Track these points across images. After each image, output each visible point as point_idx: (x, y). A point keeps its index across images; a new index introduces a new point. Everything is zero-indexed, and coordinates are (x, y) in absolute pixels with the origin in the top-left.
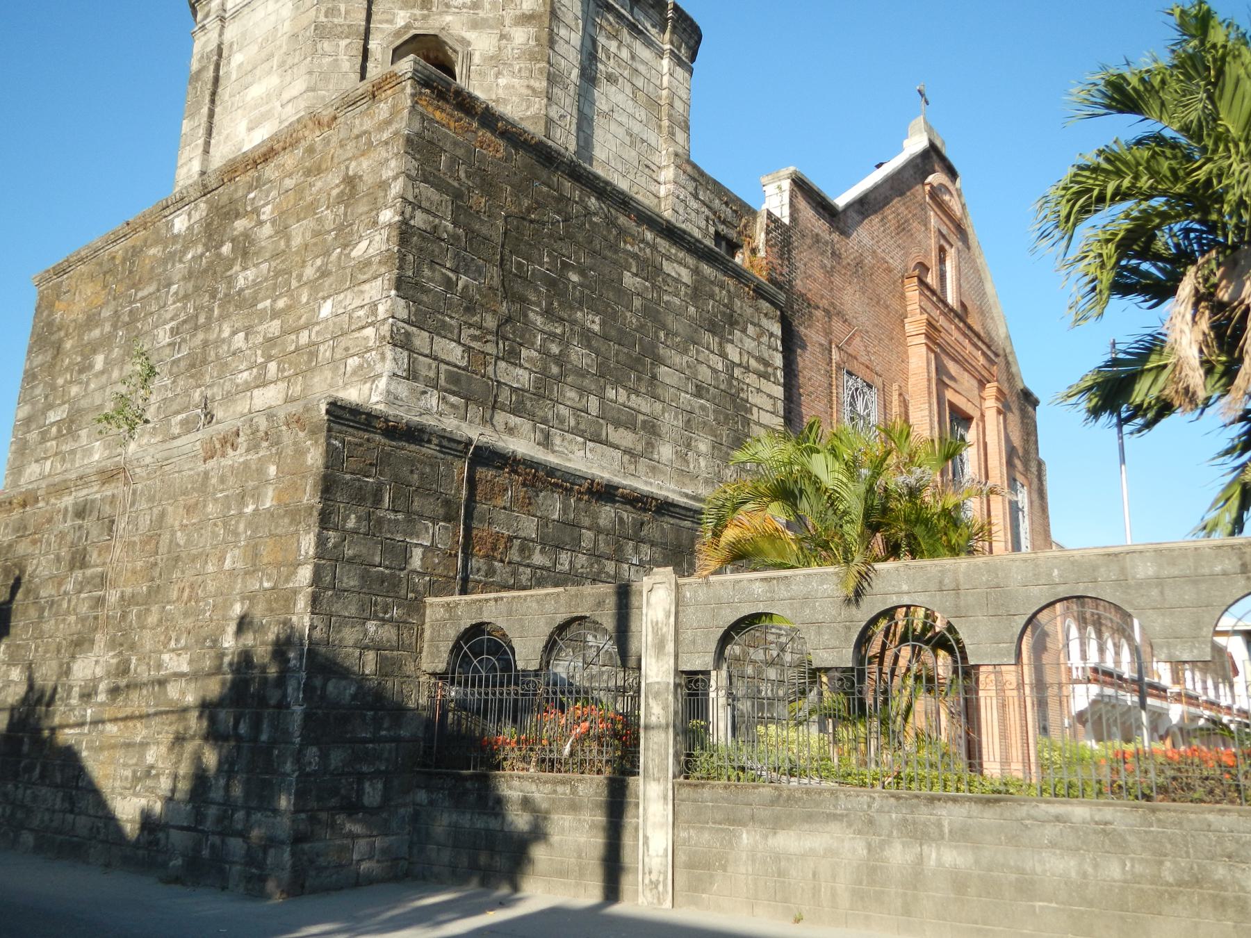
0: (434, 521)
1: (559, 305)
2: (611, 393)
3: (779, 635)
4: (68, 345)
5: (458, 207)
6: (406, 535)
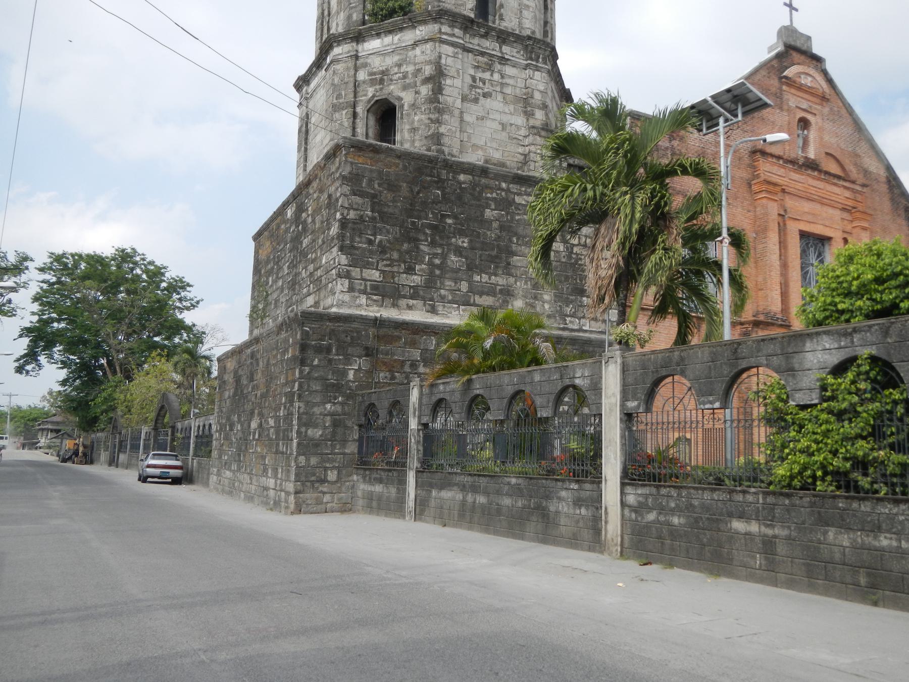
0: (360, 357)
1: (441, 238)
2: (477, 278)
4: (263, 271)
5: (374, 203)
6: (345, 364)
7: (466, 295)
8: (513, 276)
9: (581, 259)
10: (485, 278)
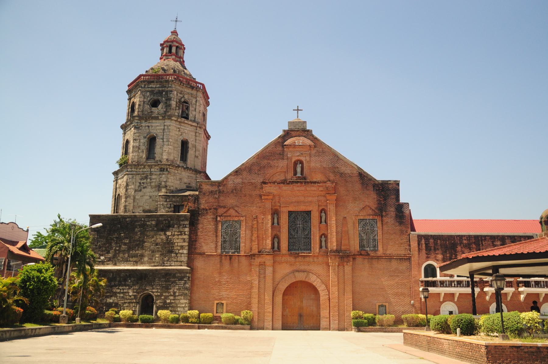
3: (174, 290)
7: (127, 258)
8: (144, 249)
9: (172, 240)
10: (134, 252)
